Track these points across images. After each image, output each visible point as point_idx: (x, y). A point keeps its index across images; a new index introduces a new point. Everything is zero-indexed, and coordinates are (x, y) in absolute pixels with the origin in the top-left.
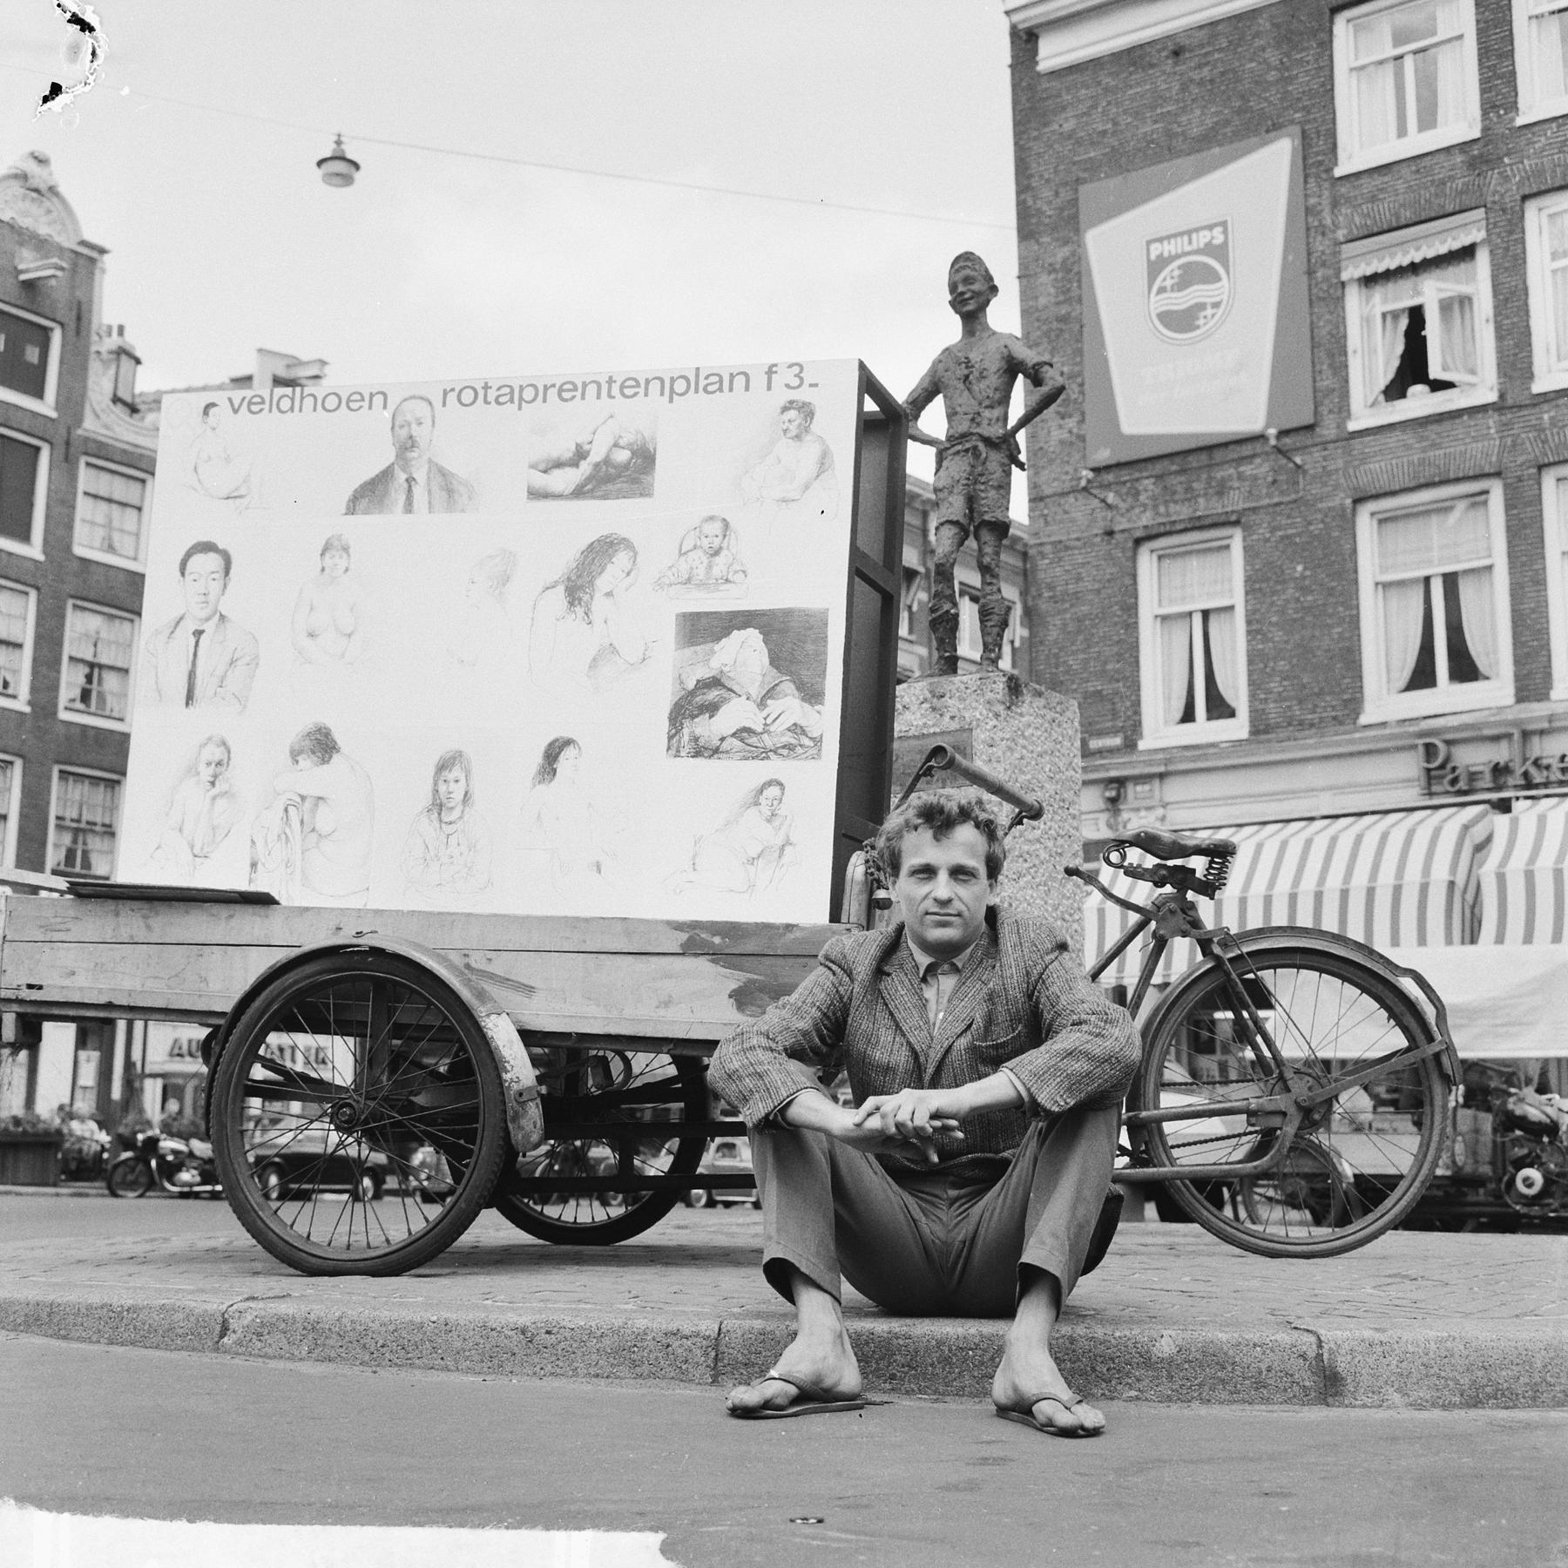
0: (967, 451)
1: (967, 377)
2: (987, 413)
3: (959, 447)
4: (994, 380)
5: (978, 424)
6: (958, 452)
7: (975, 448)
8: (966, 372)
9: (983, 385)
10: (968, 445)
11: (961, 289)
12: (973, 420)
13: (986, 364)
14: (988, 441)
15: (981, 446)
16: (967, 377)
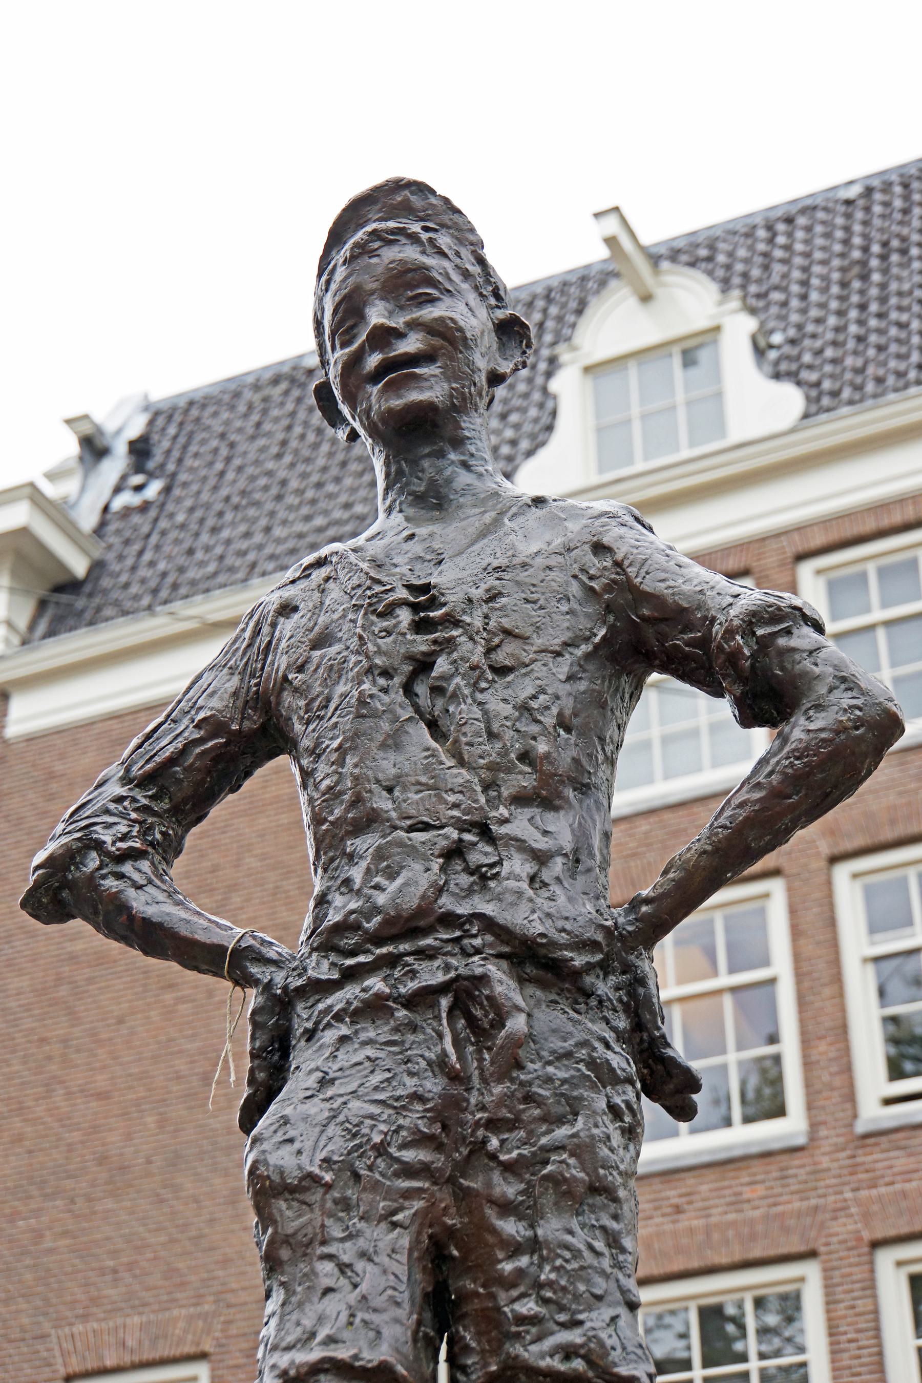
0: (422, 1000)
1: (423, 665)
2: (522, 825)
3: (376, 984)
4: (551, 681)
5: (483, 878)
6: (374, 1008)
7: (465, 993)
8: (422, 644)
9: (499, 701)
10: (432, 975)
11: (377, 315)
12: (454, 853)
13: (513, 611)
14: (534, 960)
15: (503, 983)
16: (423, 665)
